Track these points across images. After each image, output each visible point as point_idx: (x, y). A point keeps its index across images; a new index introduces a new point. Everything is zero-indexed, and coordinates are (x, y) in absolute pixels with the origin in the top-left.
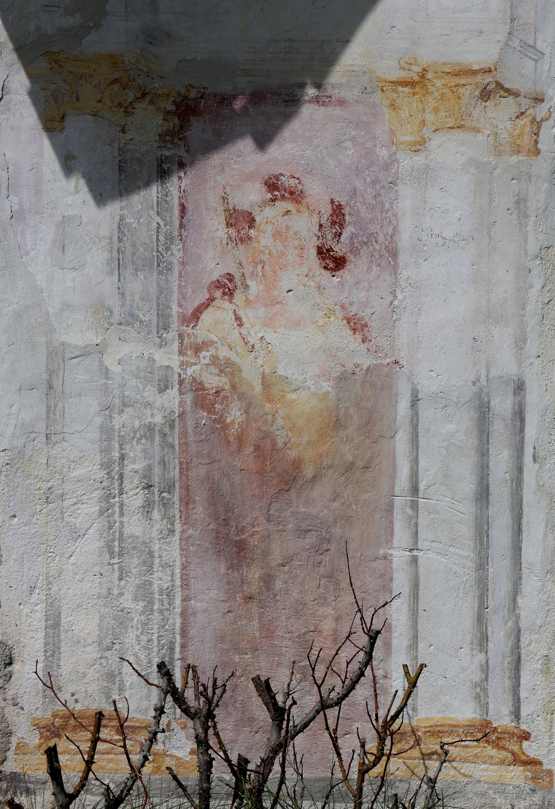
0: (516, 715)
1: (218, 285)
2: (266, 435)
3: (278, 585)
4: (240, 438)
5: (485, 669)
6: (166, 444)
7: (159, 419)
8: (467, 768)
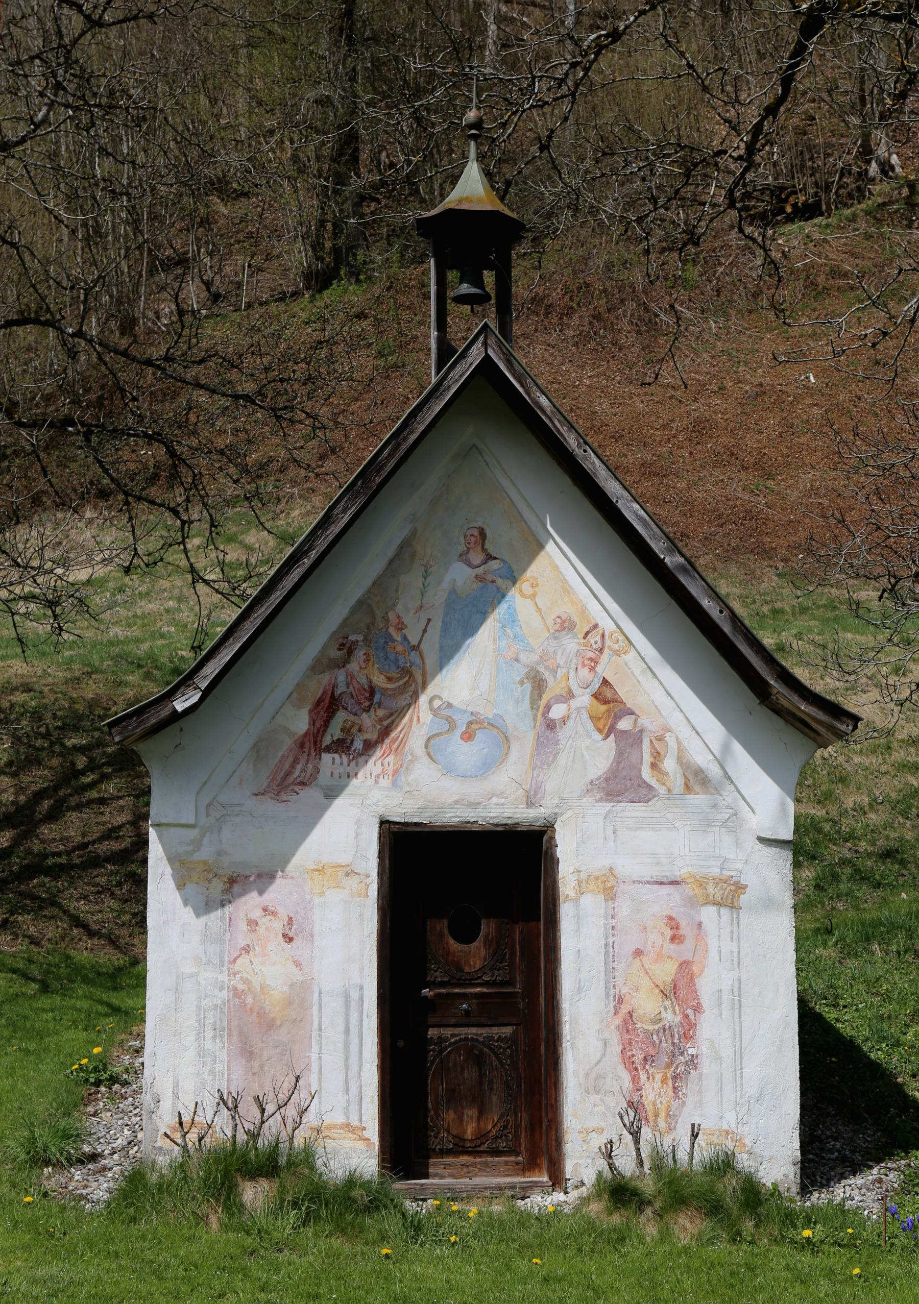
0: (361, 1120)
1: (243, 949)
2: (262, 1008)
3: (266, 1068)
4: (251, 1009)
5: (348, 1102)
6: (222, 1012)
7: (219, 1002)
8: (341, 1142)
